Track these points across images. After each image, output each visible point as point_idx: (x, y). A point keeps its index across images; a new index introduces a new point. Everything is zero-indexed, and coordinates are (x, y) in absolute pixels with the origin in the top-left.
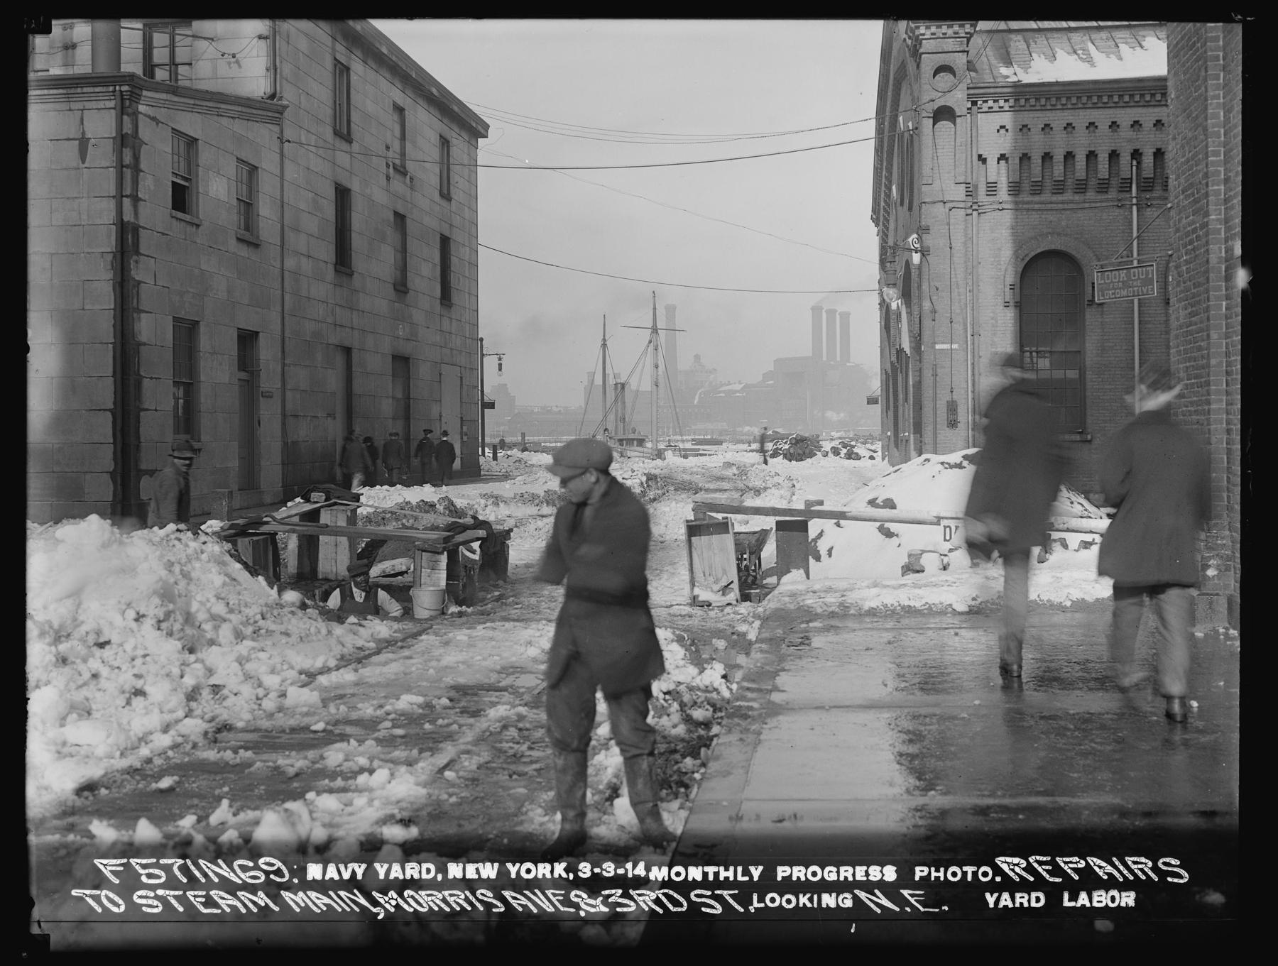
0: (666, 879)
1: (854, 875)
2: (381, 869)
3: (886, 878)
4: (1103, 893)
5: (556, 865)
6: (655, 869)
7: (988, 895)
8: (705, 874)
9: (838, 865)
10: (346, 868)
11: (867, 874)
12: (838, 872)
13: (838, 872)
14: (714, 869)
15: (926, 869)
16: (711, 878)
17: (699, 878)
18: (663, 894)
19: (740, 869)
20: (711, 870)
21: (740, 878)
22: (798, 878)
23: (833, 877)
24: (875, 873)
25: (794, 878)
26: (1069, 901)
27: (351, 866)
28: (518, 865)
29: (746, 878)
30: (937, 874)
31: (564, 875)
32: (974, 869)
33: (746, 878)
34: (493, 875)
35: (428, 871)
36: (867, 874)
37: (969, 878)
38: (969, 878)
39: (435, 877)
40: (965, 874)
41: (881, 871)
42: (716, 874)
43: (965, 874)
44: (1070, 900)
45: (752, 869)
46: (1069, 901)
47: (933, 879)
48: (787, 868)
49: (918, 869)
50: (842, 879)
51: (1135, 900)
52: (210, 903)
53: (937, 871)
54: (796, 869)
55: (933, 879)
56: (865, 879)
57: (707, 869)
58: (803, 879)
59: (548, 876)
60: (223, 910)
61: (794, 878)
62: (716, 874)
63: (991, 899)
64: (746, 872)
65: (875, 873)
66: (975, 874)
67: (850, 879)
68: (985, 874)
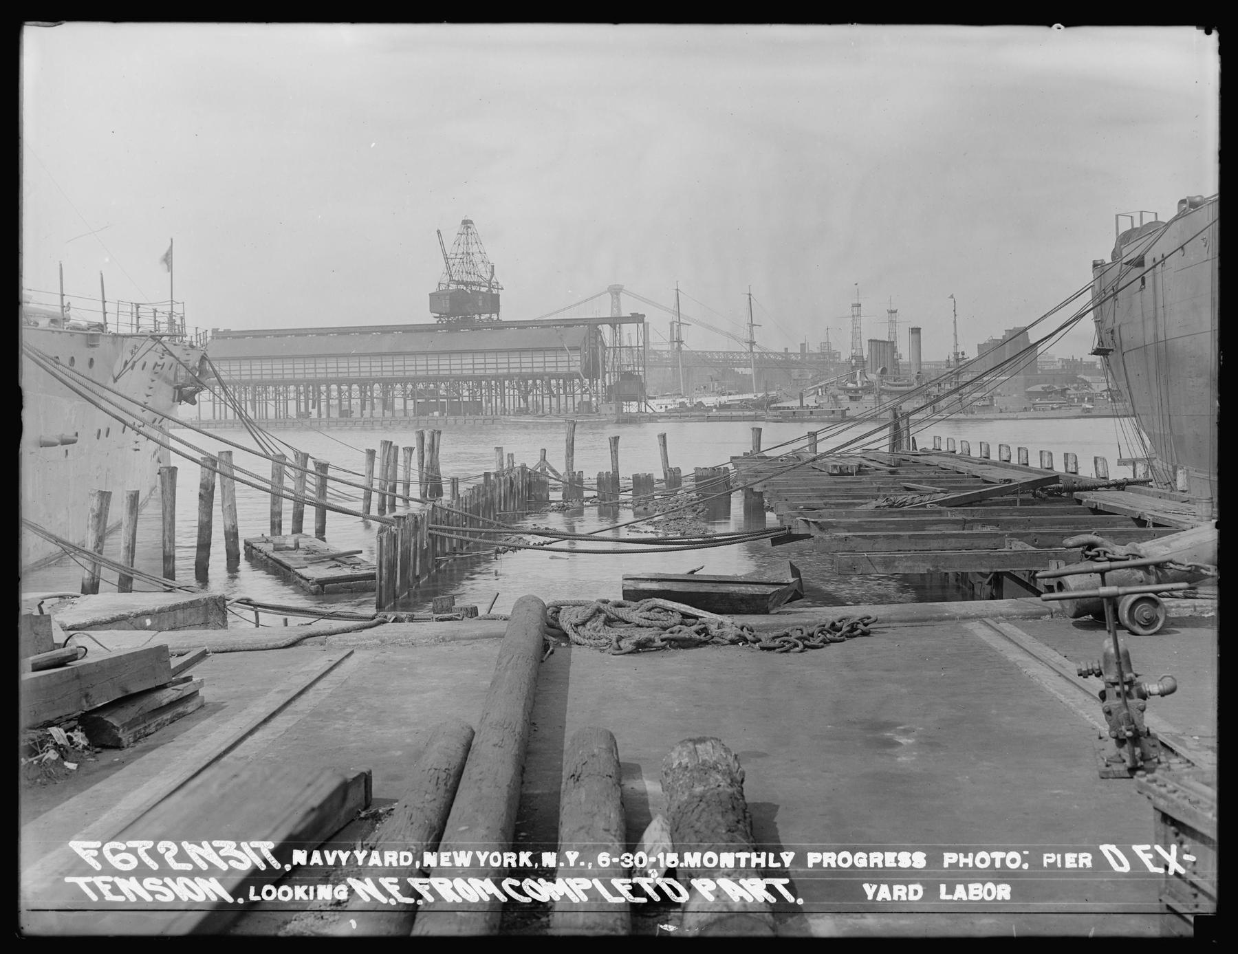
0: (699, 865)
1: (884, 861)
2: (360, 856)
3: (915, 865)
4: (979, 886)
5: (522, 854)
6: (687, 855)
7: (866, 886)
8: (737, 861)
9: (868, 851)
10: (331, 854)
11: (897, 861)
12: (868, 858)
13: (868, 858)
14: (747, 855)
15: (954, 855)
16: (743, 864)
17: (731, 865)
18: (87, 884)
19: (771, 856)
20: (743, 856)
21: (772, 865)
22: (829, 864)
23: (863, 864)
24: (905, 860)
25: (825, 865)
26: (947, 893)
27: (334, 853)
28: (487, 853)
29: (778, 865)
30: (966, 861)
31: (529, 864)
32: (1002, 855)
33: (778, 865)
34: (467, 864)
35: (406, 859)
36: (897, 861)
37: (998, 865)
38: (998, 865)
39: (414, 862)
40: (993, 860)
41: (911, 858)
42: (748, 860)
43: (993, 860)
44: (947, 893)
45: (783, 855)
46: (947, 893)
47: (961, 865)
48: (818, 855)
49: (947, 855)
50: (872, 865)
51: (1011, 893)
52: (116, 890)
53: (966, 856)
54: (826, 855)
55: (961, 865)
56: (895, 865)
57: (739, 855)
58: (834, 865)
59: (514, 865)
60: (127, 899)
61: (825, 865)
62: (748, 860)
63: (869, 890)
64: (778, 859)
65: (905, 860)
66: (1003, 860)
67: (880, 865)
68: (1013, 861)
